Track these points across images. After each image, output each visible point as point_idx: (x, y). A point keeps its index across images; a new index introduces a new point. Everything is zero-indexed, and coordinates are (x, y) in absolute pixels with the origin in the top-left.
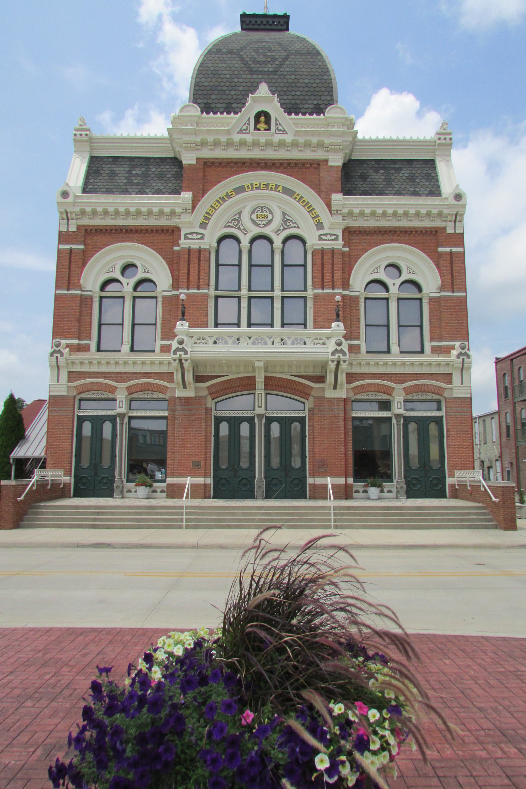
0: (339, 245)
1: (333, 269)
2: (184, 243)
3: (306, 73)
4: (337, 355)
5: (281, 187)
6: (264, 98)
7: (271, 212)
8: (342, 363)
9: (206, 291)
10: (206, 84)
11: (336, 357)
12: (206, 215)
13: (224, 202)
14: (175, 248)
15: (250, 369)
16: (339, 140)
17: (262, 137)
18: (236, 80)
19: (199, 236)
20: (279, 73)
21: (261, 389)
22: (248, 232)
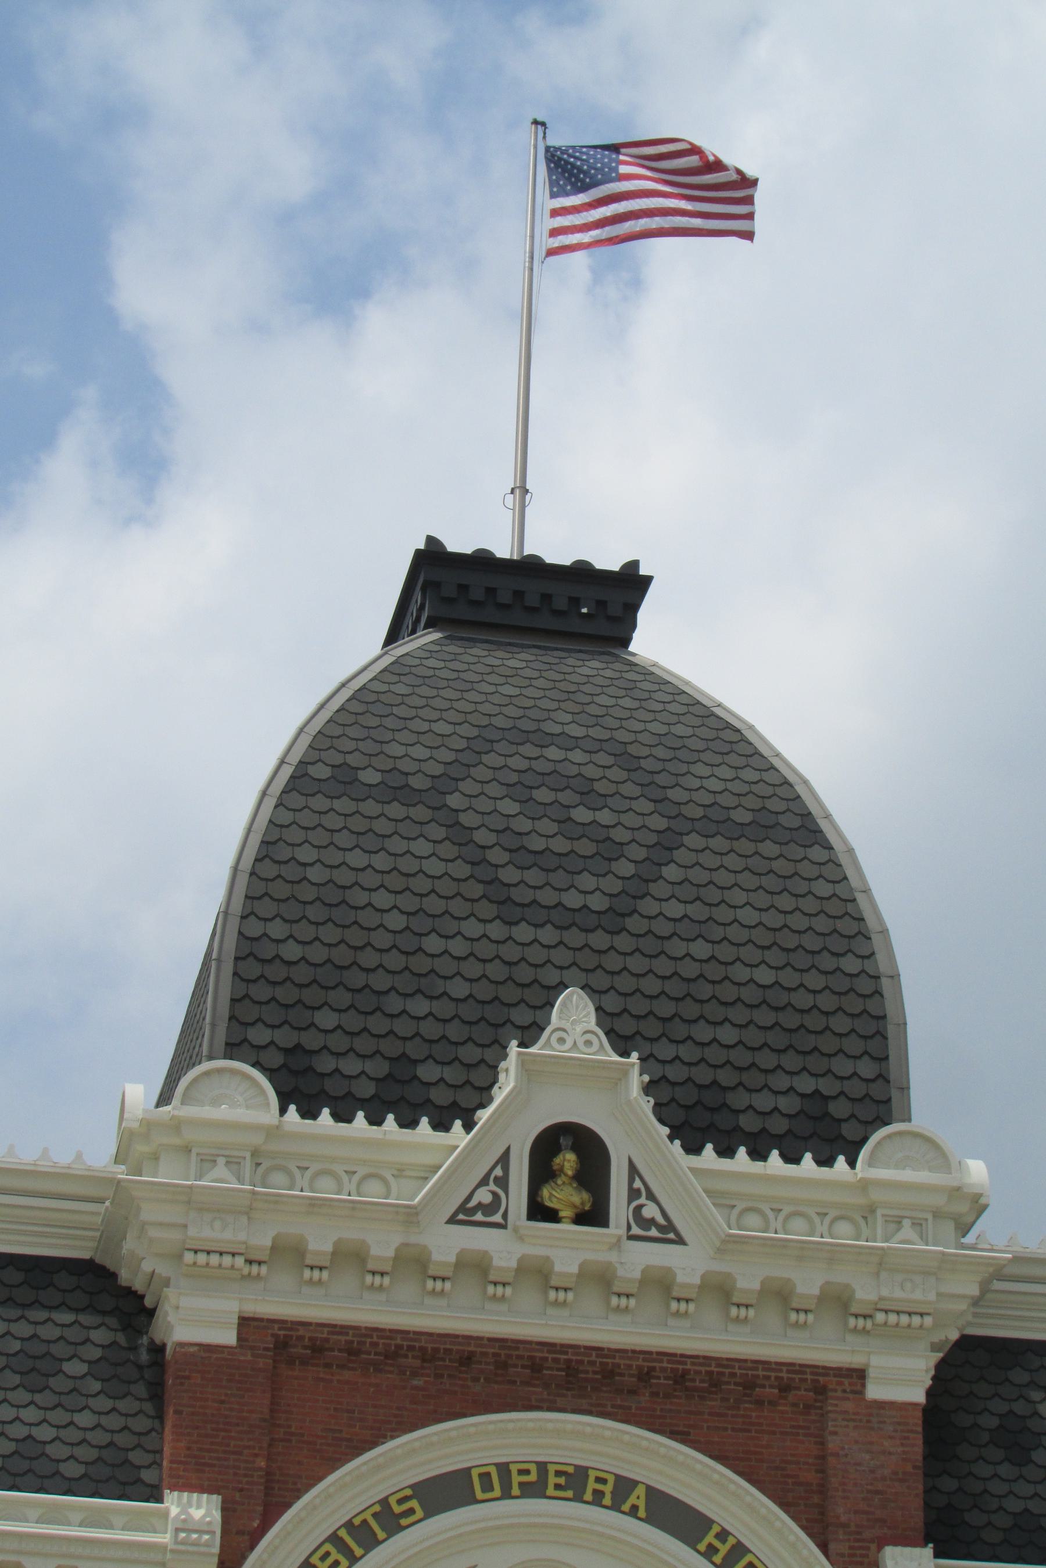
3: (762, 937)
5: (640, 1490)
6: (571, 1063)
10: (291, 951)
13: (368, 1549)
16: (922, 1294)
17: (567, 1247)
18: (433, 944)
20: (634, 923)
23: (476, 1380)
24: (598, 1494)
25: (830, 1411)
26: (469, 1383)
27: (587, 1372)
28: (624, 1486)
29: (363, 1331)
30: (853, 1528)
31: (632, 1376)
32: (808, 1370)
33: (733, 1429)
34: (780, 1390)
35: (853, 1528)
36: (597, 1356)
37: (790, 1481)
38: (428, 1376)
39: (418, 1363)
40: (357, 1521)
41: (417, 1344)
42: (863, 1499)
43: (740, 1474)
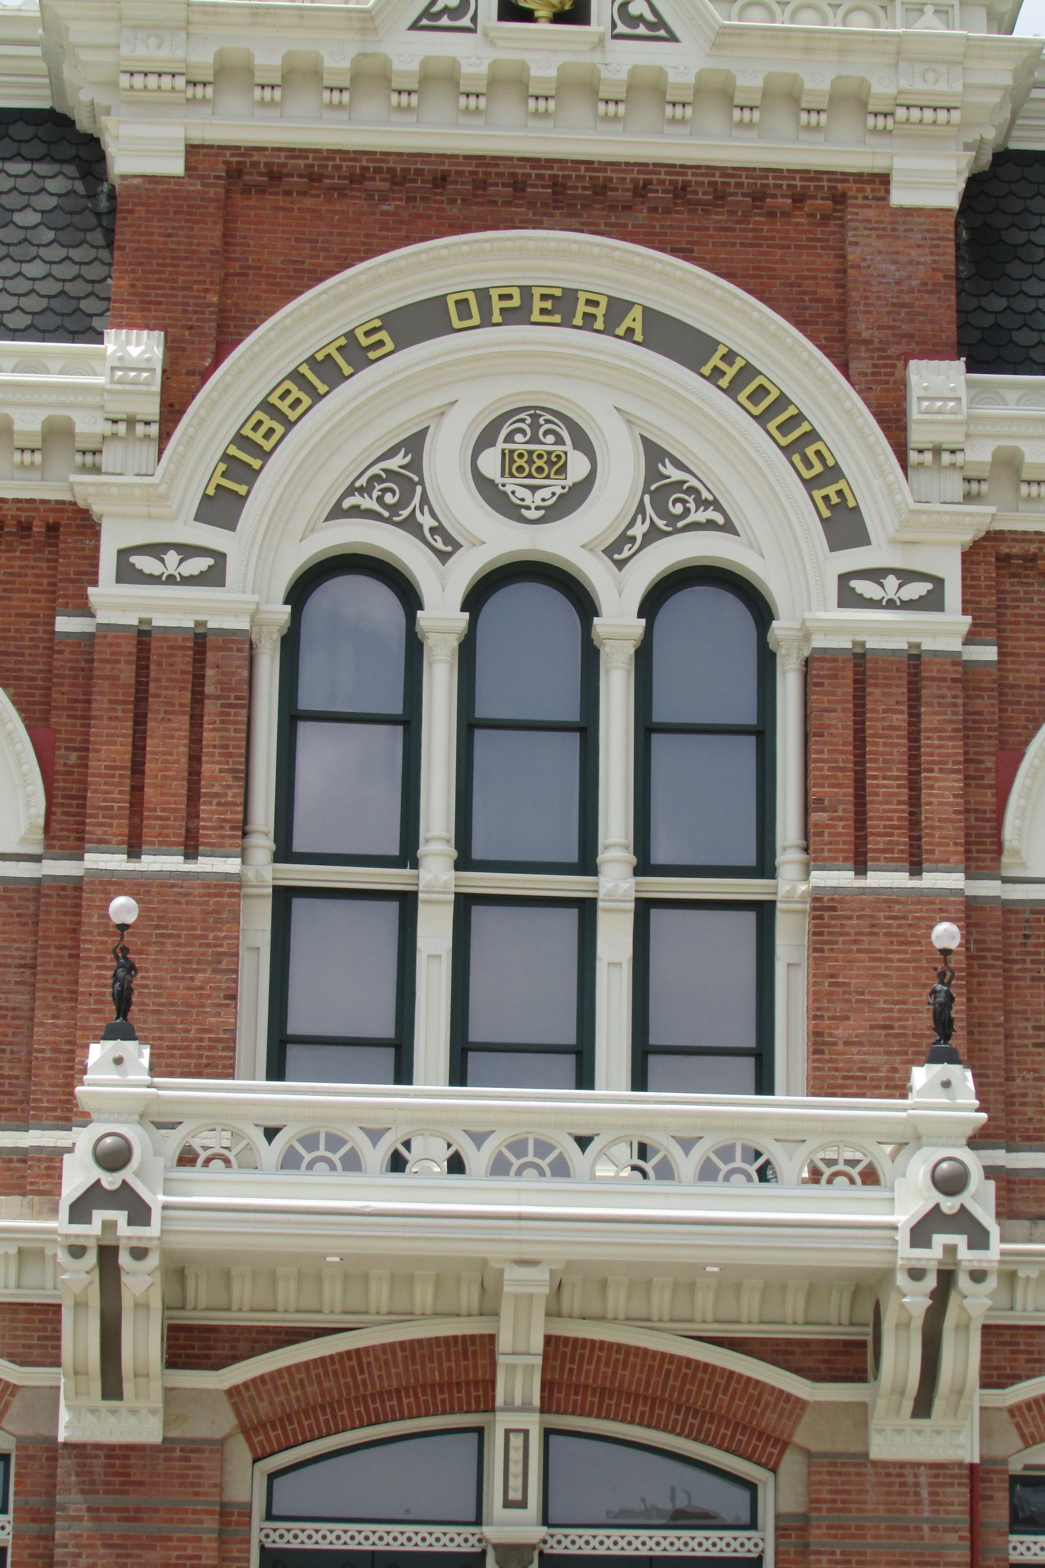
0: (946, 631)
1: (914, 757)
2: (115, 603)
4: (939, 1240)
5: (637, 312)
7: (583, 443)
8: (963, 1282)
9: (231, 865)
11: (932, 1255)
12: (233, 451)
14: (64, 624)
15: (469, 1297)
16: (945, 85)
19: (198, 565)
21: (525, 1408)
22: (457, 546)
23: (452, 202)
24: (589, 318)
25: (850, 220)
26: (445, 206)
27: (576, 188)
28: (618, 308)
29: (325, 154)
30: (876, 345)
31: (628, 190)
32: (825, 177)
33: (742, 245)
34: (794, 201)
35: (876, 345)
36: (586, 170)
37: (807, 298)
38: (400, 199)
39: (386, 185)
40: (320, 357)
41: (385, 166)
42: (888, 313)
43: (750, 292)
